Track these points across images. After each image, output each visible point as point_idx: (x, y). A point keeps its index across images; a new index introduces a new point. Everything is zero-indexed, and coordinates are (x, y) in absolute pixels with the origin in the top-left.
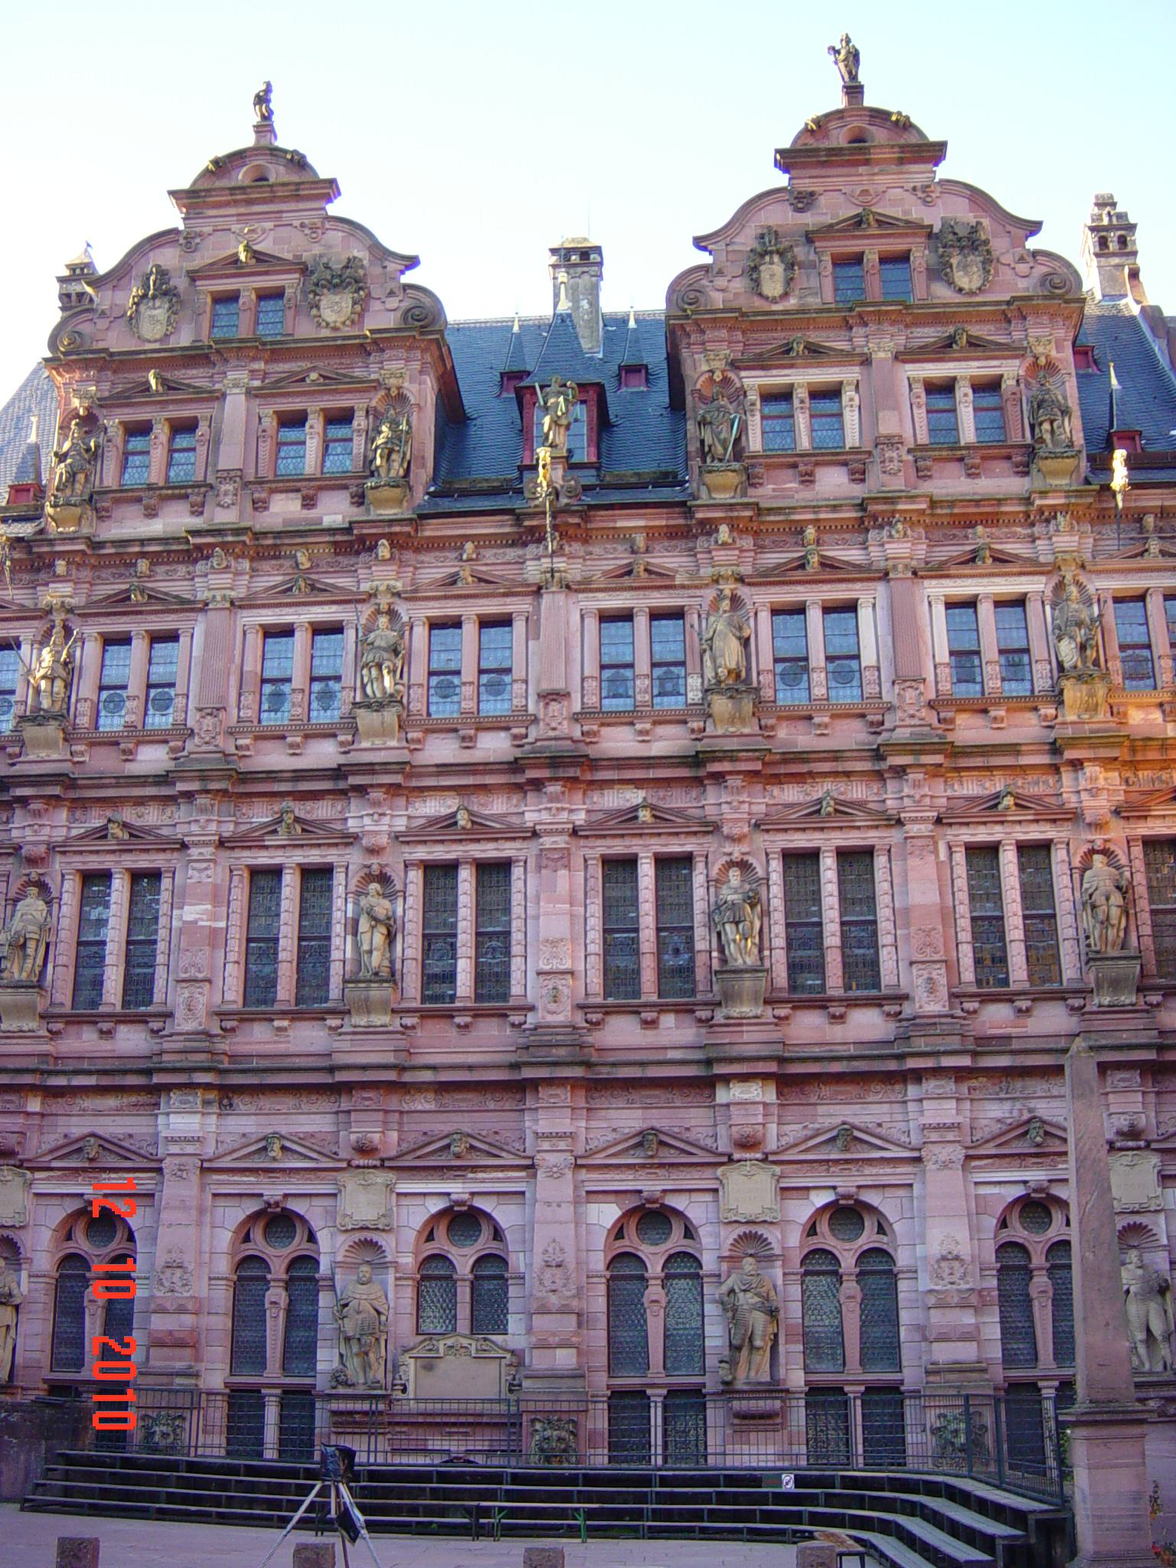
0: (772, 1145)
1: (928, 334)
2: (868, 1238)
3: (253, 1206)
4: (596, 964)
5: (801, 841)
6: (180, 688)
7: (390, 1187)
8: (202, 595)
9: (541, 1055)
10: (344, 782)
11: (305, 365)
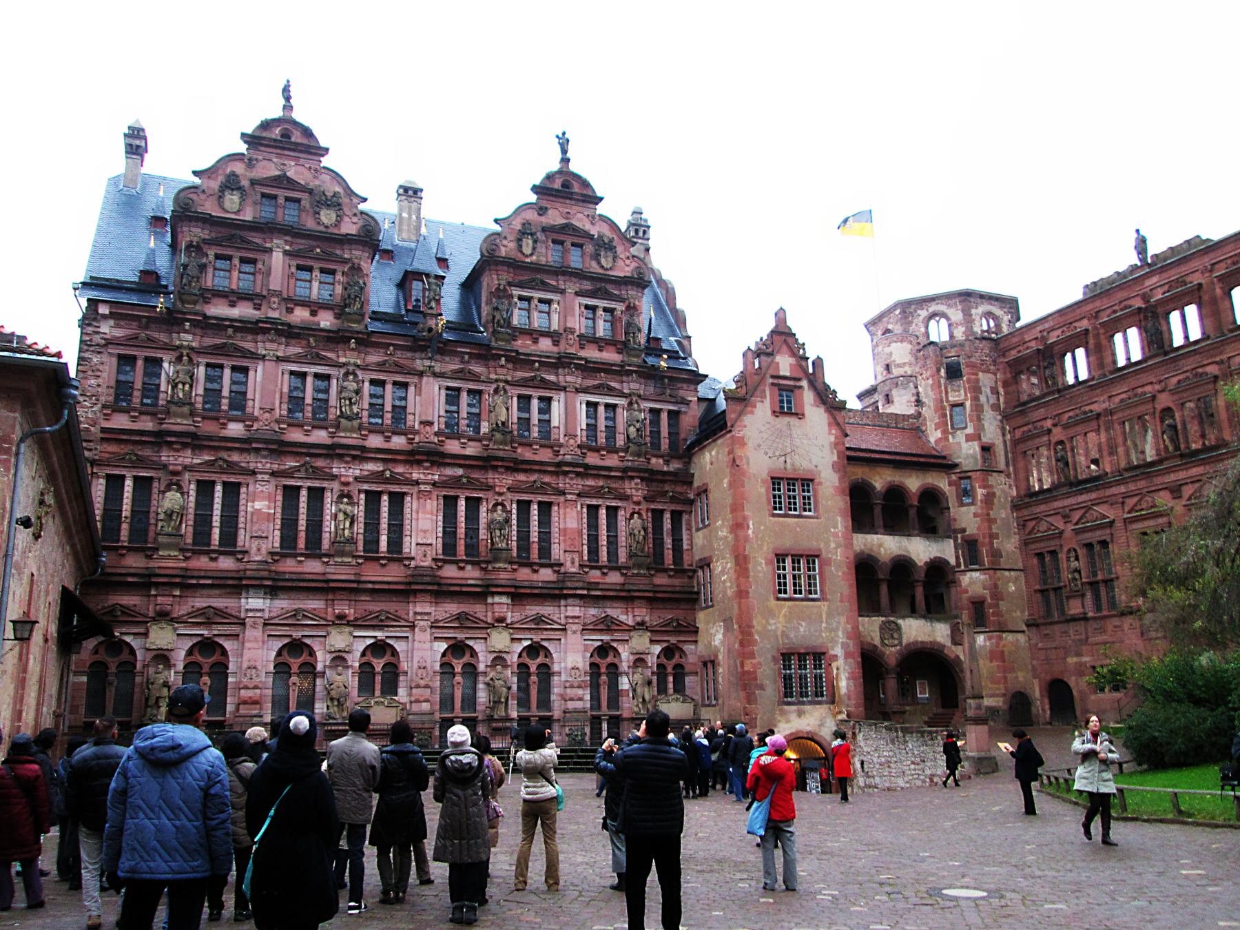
0: (509, 621)
1: (587, 286)
2: (540, 660)
3: (287, 640)
4: (440, 540)
5: (525, 497)
6: (249, 396)
7: (351, 633)
9: (419, 580)
10: (334, 452)
11: (314, 243)
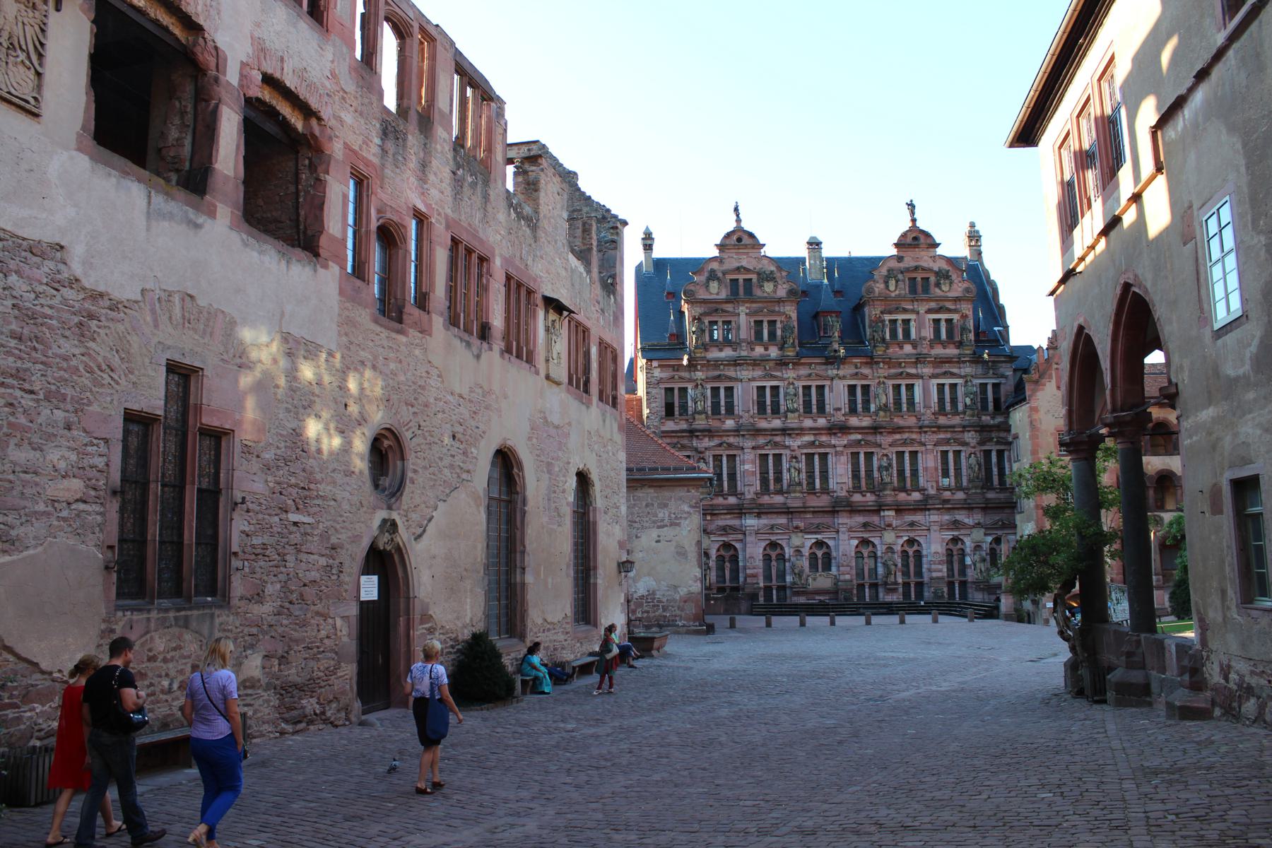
1: (933, 305)
2: (915, 548)
5: (901, 449)
8: (740, 376)
10: (785, 431)
